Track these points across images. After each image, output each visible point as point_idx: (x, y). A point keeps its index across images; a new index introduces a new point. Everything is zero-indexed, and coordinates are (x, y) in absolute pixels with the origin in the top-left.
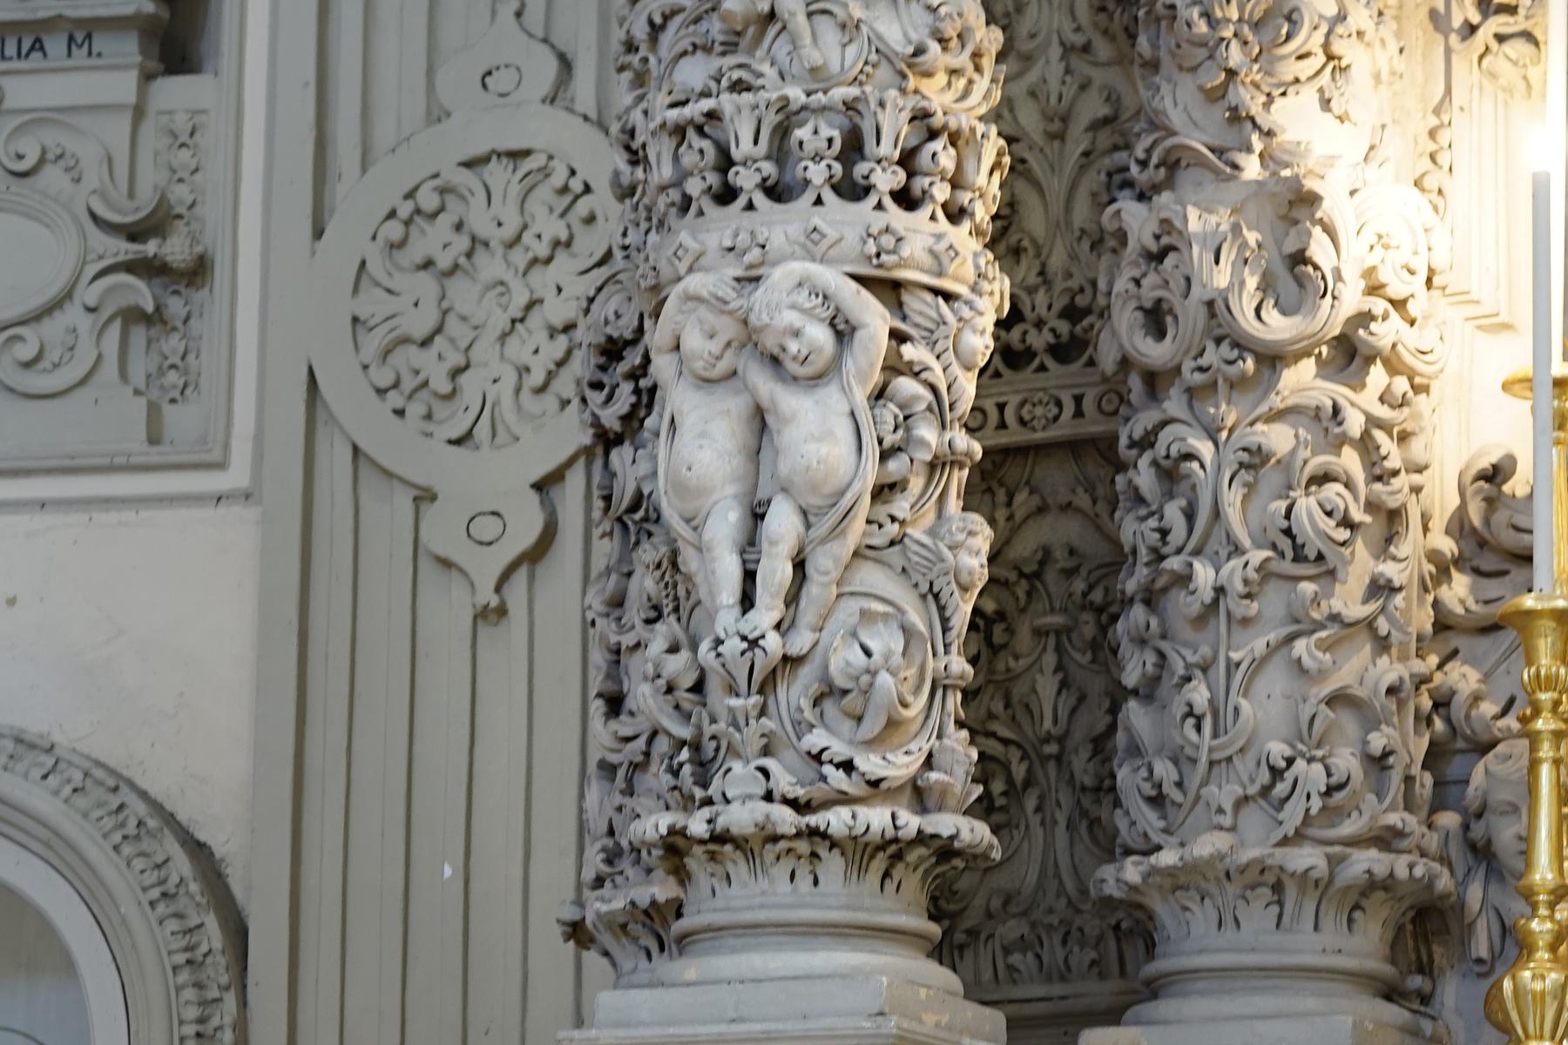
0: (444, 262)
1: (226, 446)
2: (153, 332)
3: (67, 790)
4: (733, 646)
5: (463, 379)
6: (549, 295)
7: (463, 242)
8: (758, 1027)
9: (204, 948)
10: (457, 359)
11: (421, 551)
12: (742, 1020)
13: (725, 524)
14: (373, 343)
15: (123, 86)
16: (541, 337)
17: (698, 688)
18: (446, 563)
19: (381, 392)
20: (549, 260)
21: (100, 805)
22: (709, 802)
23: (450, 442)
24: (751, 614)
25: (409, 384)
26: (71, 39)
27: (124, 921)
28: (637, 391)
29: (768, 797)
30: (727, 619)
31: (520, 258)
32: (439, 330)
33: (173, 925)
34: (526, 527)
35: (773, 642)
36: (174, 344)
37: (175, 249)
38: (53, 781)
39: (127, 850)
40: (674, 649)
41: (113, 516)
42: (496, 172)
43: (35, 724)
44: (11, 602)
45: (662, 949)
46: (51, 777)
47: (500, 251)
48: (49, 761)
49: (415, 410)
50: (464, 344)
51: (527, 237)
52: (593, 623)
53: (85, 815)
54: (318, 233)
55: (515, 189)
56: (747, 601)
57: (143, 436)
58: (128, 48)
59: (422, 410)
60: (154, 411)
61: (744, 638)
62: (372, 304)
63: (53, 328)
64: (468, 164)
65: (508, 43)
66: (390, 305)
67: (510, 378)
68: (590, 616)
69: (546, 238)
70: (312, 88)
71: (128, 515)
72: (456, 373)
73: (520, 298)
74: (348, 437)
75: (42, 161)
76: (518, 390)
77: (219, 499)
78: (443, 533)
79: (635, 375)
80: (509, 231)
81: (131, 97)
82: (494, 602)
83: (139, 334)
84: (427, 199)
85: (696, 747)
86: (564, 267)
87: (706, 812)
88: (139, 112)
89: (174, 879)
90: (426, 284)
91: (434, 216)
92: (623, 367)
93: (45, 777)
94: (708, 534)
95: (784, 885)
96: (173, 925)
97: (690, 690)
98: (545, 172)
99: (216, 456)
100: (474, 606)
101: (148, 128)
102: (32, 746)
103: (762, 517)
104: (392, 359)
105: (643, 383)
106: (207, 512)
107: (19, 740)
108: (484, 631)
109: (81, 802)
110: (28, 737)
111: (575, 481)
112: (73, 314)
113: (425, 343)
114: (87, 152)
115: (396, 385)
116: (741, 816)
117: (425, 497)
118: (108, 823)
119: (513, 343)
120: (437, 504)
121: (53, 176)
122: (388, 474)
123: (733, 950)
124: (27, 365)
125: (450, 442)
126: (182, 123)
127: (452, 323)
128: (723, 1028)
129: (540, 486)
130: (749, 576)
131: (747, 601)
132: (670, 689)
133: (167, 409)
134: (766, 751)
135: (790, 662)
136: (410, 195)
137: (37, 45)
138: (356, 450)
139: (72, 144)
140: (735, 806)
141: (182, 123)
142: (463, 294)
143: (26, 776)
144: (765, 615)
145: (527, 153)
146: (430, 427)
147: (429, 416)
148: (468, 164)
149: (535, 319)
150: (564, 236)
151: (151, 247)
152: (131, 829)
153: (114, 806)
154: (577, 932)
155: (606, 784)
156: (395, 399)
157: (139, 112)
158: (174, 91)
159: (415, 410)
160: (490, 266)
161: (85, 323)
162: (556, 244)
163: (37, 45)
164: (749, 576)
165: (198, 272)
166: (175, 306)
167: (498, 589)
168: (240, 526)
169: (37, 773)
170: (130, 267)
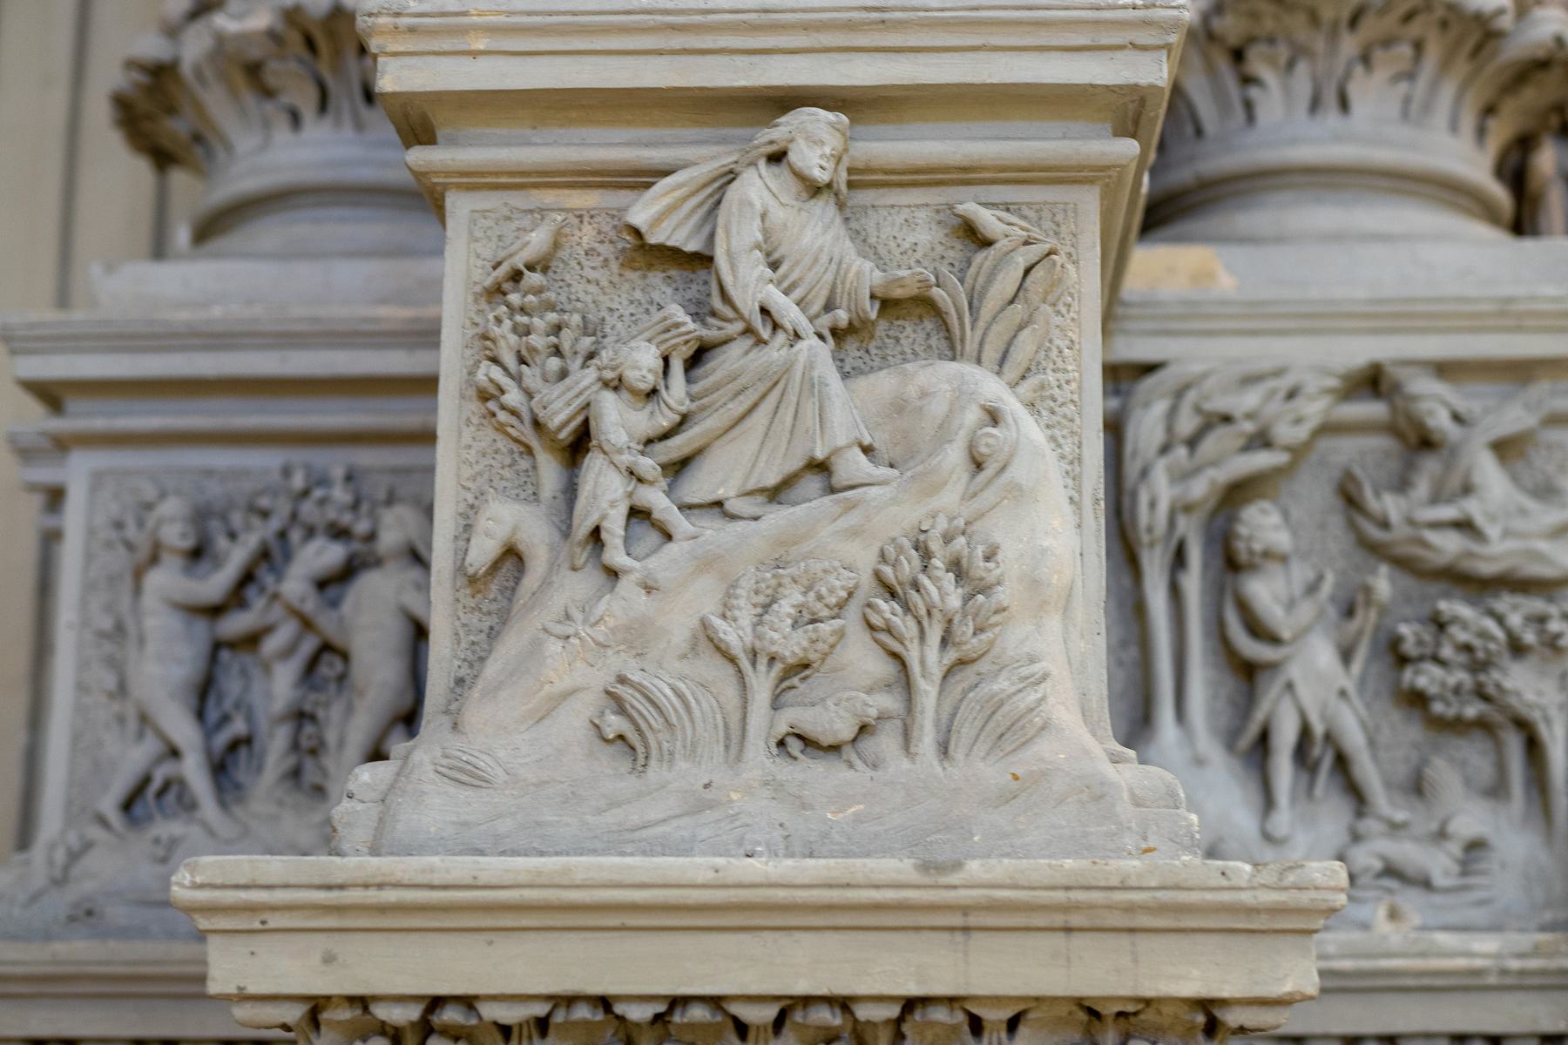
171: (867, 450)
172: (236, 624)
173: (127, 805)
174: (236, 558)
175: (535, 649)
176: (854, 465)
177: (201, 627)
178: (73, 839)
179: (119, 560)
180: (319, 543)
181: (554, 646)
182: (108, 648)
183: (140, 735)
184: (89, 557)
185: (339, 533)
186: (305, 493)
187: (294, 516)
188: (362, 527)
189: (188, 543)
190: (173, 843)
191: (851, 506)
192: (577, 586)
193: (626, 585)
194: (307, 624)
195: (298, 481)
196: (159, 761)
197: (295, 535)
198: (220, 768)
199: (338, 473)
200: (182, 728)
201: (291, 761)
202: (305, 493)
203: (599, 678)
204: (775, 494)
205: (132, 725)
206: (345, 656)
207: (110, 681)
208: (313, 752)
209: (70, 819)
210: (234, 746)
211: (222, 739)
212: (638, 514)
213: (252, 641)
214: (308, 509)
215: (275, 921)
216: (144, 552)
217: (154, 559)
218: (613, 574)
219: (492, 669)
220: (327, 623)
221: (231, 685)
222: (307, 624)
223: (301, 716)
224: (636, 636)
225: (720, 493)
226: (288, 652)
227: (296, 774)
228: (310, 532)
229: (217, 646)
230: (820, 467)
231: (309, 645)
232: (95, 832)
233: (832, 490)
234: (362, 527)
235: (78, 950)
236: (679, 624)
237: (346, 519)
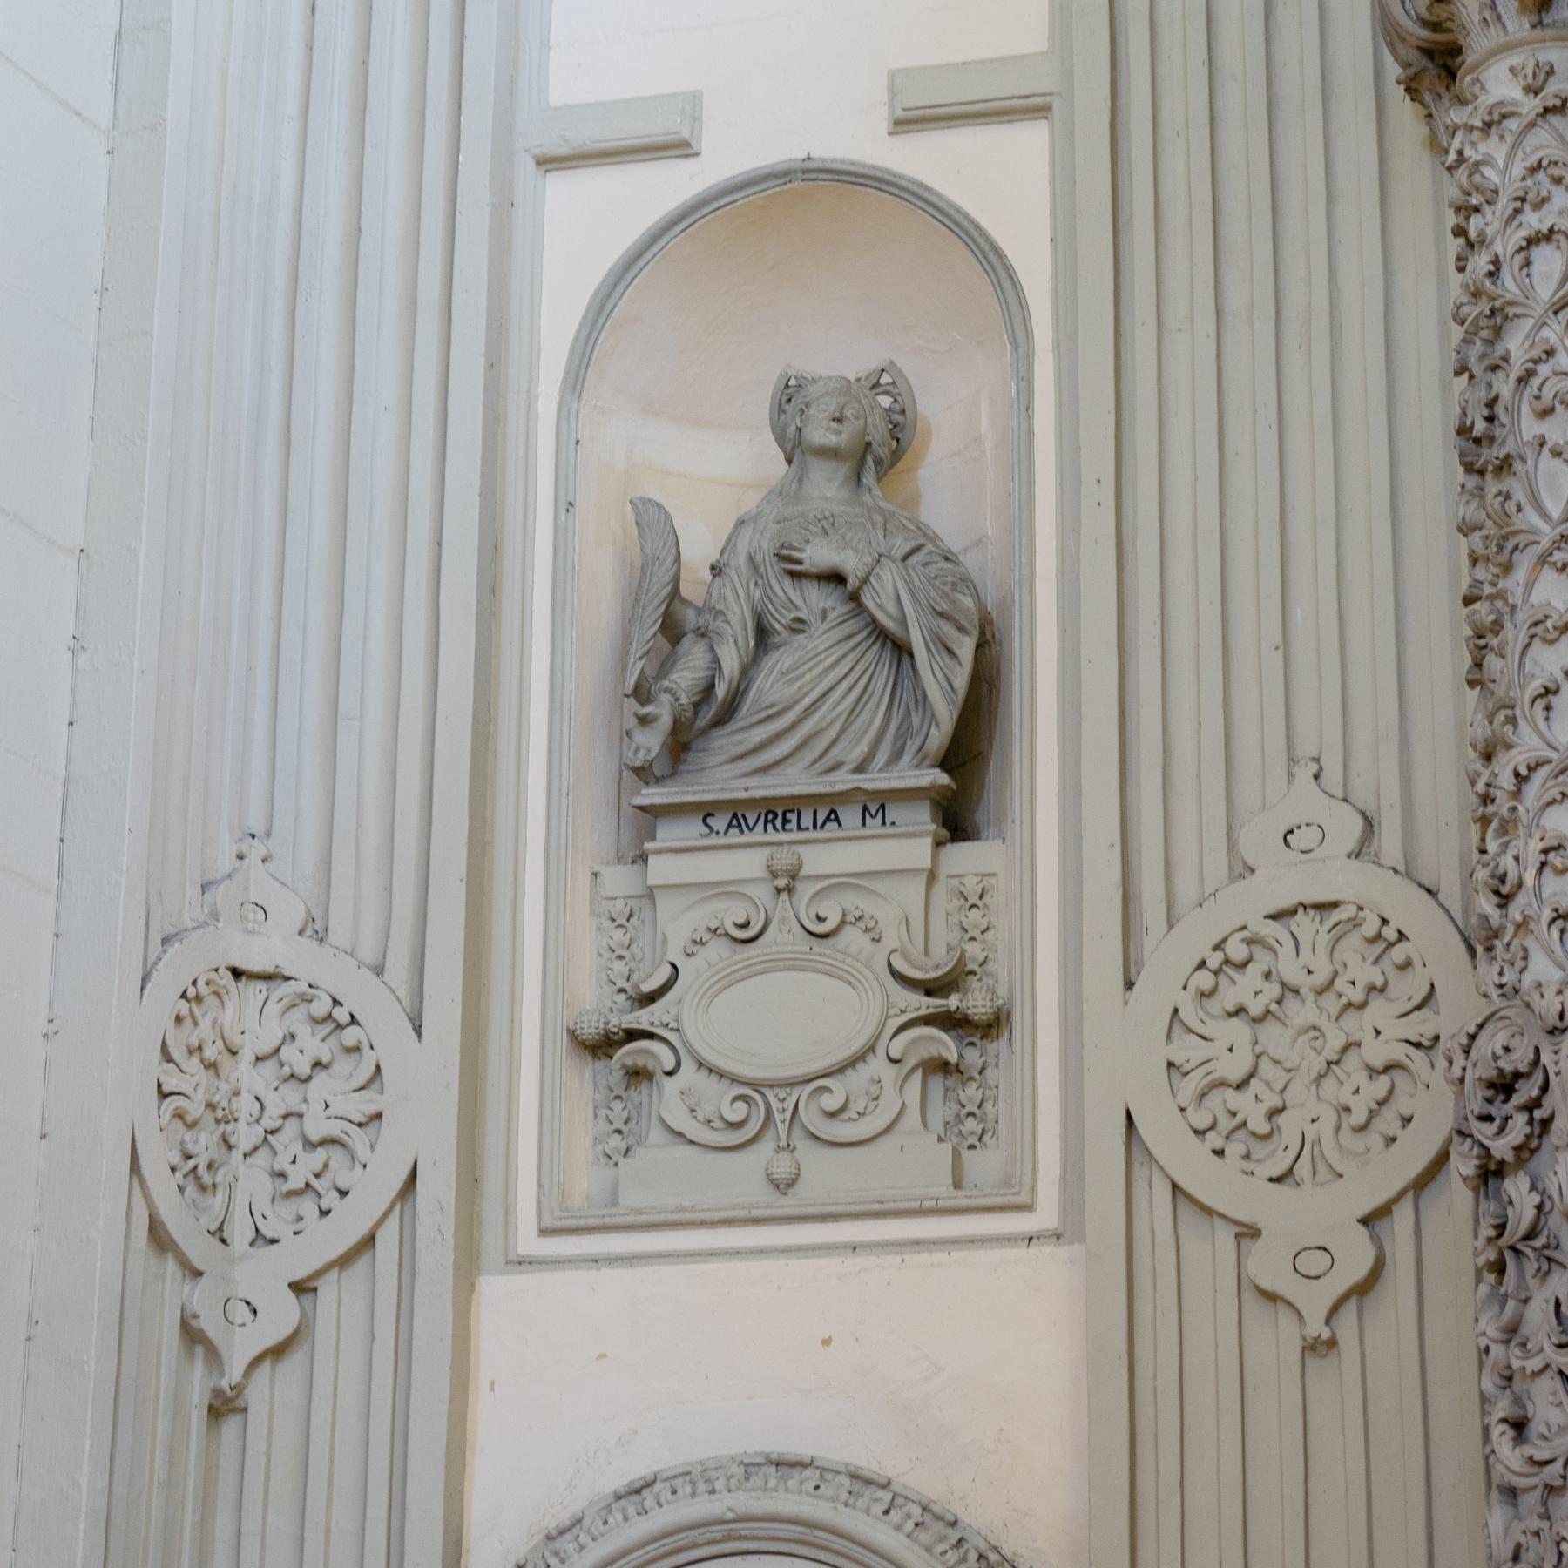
0: (1256, 1009)
1: (1033, 1189)
2: (951, 1082)
3: (909, 1525)
5: (1282, 1119)
6: (1368, 1038)
7: (1273, 990)
10: (1273, 1101)
11: (1244, 1285)
14: (1190, 1086)
15: (919, 852)
16: (1361, 1078)
18: (1271, 1297)
19: (1200, 1133)
20: (1363, 1006)
21: (942, 1539)
23: (1271, 1180)
25: (1225, 1124)
26: (865, 809)
28: (1531, 1122)
31: (1331, 1003)
32: (1252, 1075)
34: (1355, 1261)
36: (971, 1093)
37: (975, 1002)
38: (895, 1516)
41: (925, 1257)
42: (1304, 924)
43: (868, 1463)
44: (826, 1342)
46: (892, 1512)
47: (1310, 997)
48: (887, 1497)
49: (1234, 1149)
50: (1278, 1086)
51: (1340, 984)
53: (928, 1550)
54: (1129, 985)
55: (1324, 939)
57: (950, 1181)
58: (922, 818)
59: (1242, 1150)
60: (956, 1155)
62: (1187, 1050)
63: (858, 1078)
64: (1273, 917)
65: (1306, 802)
66: (1206, 1050)
67: (1329, 1118)
69: (1361, 985)
70: (1117, 850)
71: (940, 1256)
72: (1275, 1112)
73: (1335, 1041)
74: (1168, 1176)
75: (843, 922)
76: (1338, 1128)
77: (1030, 1239)
78: (1269, 1267)
79: (1530, 1107)
80: (1320, 978)
81: (927, 864)
82: (1326, 1334)
83: (937, 1084)
84: (1237, 951)
86: (1378, 1011)
88: (932, 876)
90: (1239, 1029)
91: (1243, 966)
92: (1517, 1099)
93: (886, 1512)
98: (1355, 923)
99: (1024, 1198)
100: (1304, 1339)
101: (940, 889)
102: (869, 1482)
104: (1206, 1102)
105: (1537, 1114)
106: (1020, 1252)
107: (855, 1476)
108: (1311, 1363)
109: (924, 1536)
110: (865, 1474)
111: (1403, 1216)
112: (876, 1065)
113: (1241, 1085)
114: (885, 914)
115: (1213, 1127)
117: (1248, 1233)
119: (1329, 1084)
120: (1261, 1241)
121: (853, 938)
122: (1208, 1211)
124: (832, 1115)
125: (1271, 1180)
126: (971, 885)
127: (1265, 1066)
129: (1365, 1221)
133: (965, 1153)
136: (1218, 947)
137: (833, 816)
138: (1175, 1187)
139: (868, 906)
141: (971, 885)
142: (1274, 1038)
143: (867, 1511)
145: (1334, 905)
146: (1250, 1166)
147: (1247, 1156)
148: (1273, 917)
149: (1352, 1061)
150: (1379, 982)
151: (953, 1002)
153: (954, 1541)
156: (1214, 1139)
157: (932, 876)
158: (961, 856)
159: (1234, 1149)
160: (1301, 1012)
161: (889, 1074)
162: (1372, 988)
163: (833, 816)
165: (993, 1026)
166: (973, 1057)
167: (1327, 1322)
168: (1053, 1263)
169: (878, 1509)
170: (927, 1021)
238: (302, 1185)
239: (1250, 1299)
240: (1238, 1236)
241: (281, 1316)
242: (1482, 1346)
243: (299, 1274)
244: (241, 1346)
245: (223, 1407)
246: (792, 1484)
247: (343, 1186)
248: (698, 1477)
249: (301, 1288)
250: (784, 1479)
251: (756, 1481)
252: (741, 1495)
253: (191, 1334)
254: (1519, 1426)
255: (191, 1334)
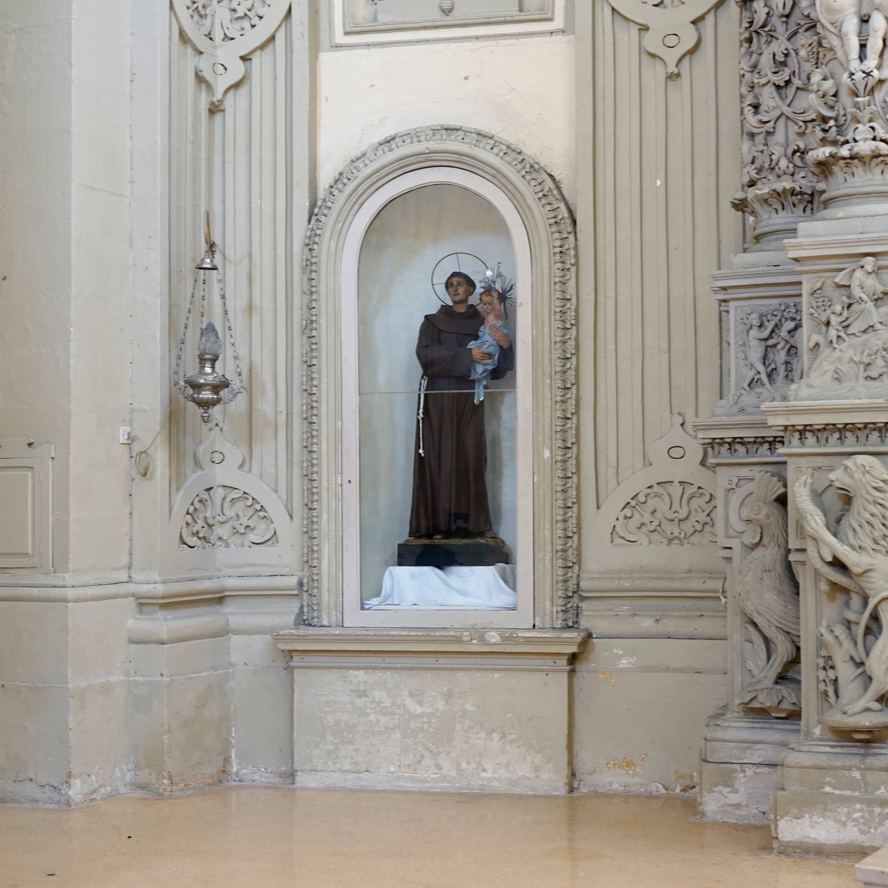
1: (553, 11)
3: (501, 154)
4: (859, 76)
8: (876, 235)
9: (560, 217)
11: (642, 51)
12: (866, 233)
13: (851, 25)
17: (835, 95)
18: (653, 56)
21: (515, 159)
22: (847, 142)
23: (654, 5)
24: (865, 62)
27: (528, 206)
29: (874, 139)
30: (855, 65)
33: (548, 208)
34: (689, 40)
35: (876, 73)
38: (495, 150)
39: (528, 177)
40: (825, 79)
41: (507, 42)
45: (783, 209)
46: (494, 148)
48: (492, 142)
52: (744, 76)
56: (862, 58)
57: (517, 9)
61: (864, 72)
68: (742, 72)
71: (514, 41)
74: (610, 5)
77: (552, 33)
78: (652, 43)
82: (676, 71)
85: (836, 119)
87: (847, 146)
89: (547, 189)
93: (492, 148)
94: (844, 29)
95: (879, 177)
96: (548, 208)
97: (833, 96)
99: (549, 16)
100: (667, 73)
102: (485, 136)
103: (866, 21)
106: (547, 39)
107: (479, 134)
108: (670, 84)
109: (507, 158)
110: (483, 133)
111: (710, 19)
116: (865, 147)
117: (644, 28)
118: (519, 166)
120: (649, 32)
122: (627, 19)
123: (858, 204)
125: (654, 5)
128: (860, 236)
129: (693, 23)
130: (863, 46)
131: (862, 58)
132: (823, 96)
134: (870, 121)
135: (881, 82)
138: (613, 9)
140: (861, 143)
143: (484, 148)
144: (871, 63)
152: (528, 169)
153: (520, 160)
154: (741, 206)
155: (751, 142)
164: (863, 46)
167: (677, 66)
169: (488, 147)
171: (881, 323)
172: (771, 342)
173: (749, 385)
174: (770, 326)
175: (821, 363)
176: (878, 326)
177: (763, 343)
178: (738, 393)
179: (743, 328)
180: (789, 322)
181: (825, 362)
182: (742, 348)
183: (751, 369)
184: (736, 327)
185: (793, 319)
186: (785, 310)
187: (782, 316)
188: (798, 318)
189: (758, 324)
190: (761, 393)
191: (877, 334)
192: (828, 351)
193: (837, 351)
194: (787, 342)
195: (783, 308)
196: (755, 375)
197: (783, 320)
198: (769, 376)
199: (792, 304)
200: (761, 368)
201: (786, 373)
202: (785, 310)
203: (832, 368)
204: (864, 332)
205: (749, 366)
206: (796, 348)
207: (743, 357)
208: (790, 371)
209: (737, 389)
210: (773, 370)
211: (769, 369)
212: (839, 337)
213: (775, 345)
214: (785, 314)
215: (778, 413)
216: (749, 327)
217: (751, 328)
218: (835, 348)
219: (814, 366)
220: (792, 341)
221: (771, 356)
222: (787, 342)
223: (787, 363)
224: (839, 360)
225: (854, 332)
226: (783, 348)
227: (787, 376)
228: (786, 319)
229: (767, 347)
230: (872, 326)
231: (788, 346)
232: (743, 391)
233: (875, 331)
234: (798, 318)
235: (741, 418)
236: (846, 357)
237: (794, 316)
238: (243, 15)
239: (646, 59)
240: (640, 30)
241: (237, 70)
242: (742, 74)
243: (243, 53)
244: (221, 83)
245: (215, 109)
246: (452, 137)
247: (260, 15)
248: (413, 135)
249: (245, 59)
250: (449, 136)
251: (438, 136)
252: (431, 142)
253: (200, 79)
254: (756, 107)
255: (200, 79)
